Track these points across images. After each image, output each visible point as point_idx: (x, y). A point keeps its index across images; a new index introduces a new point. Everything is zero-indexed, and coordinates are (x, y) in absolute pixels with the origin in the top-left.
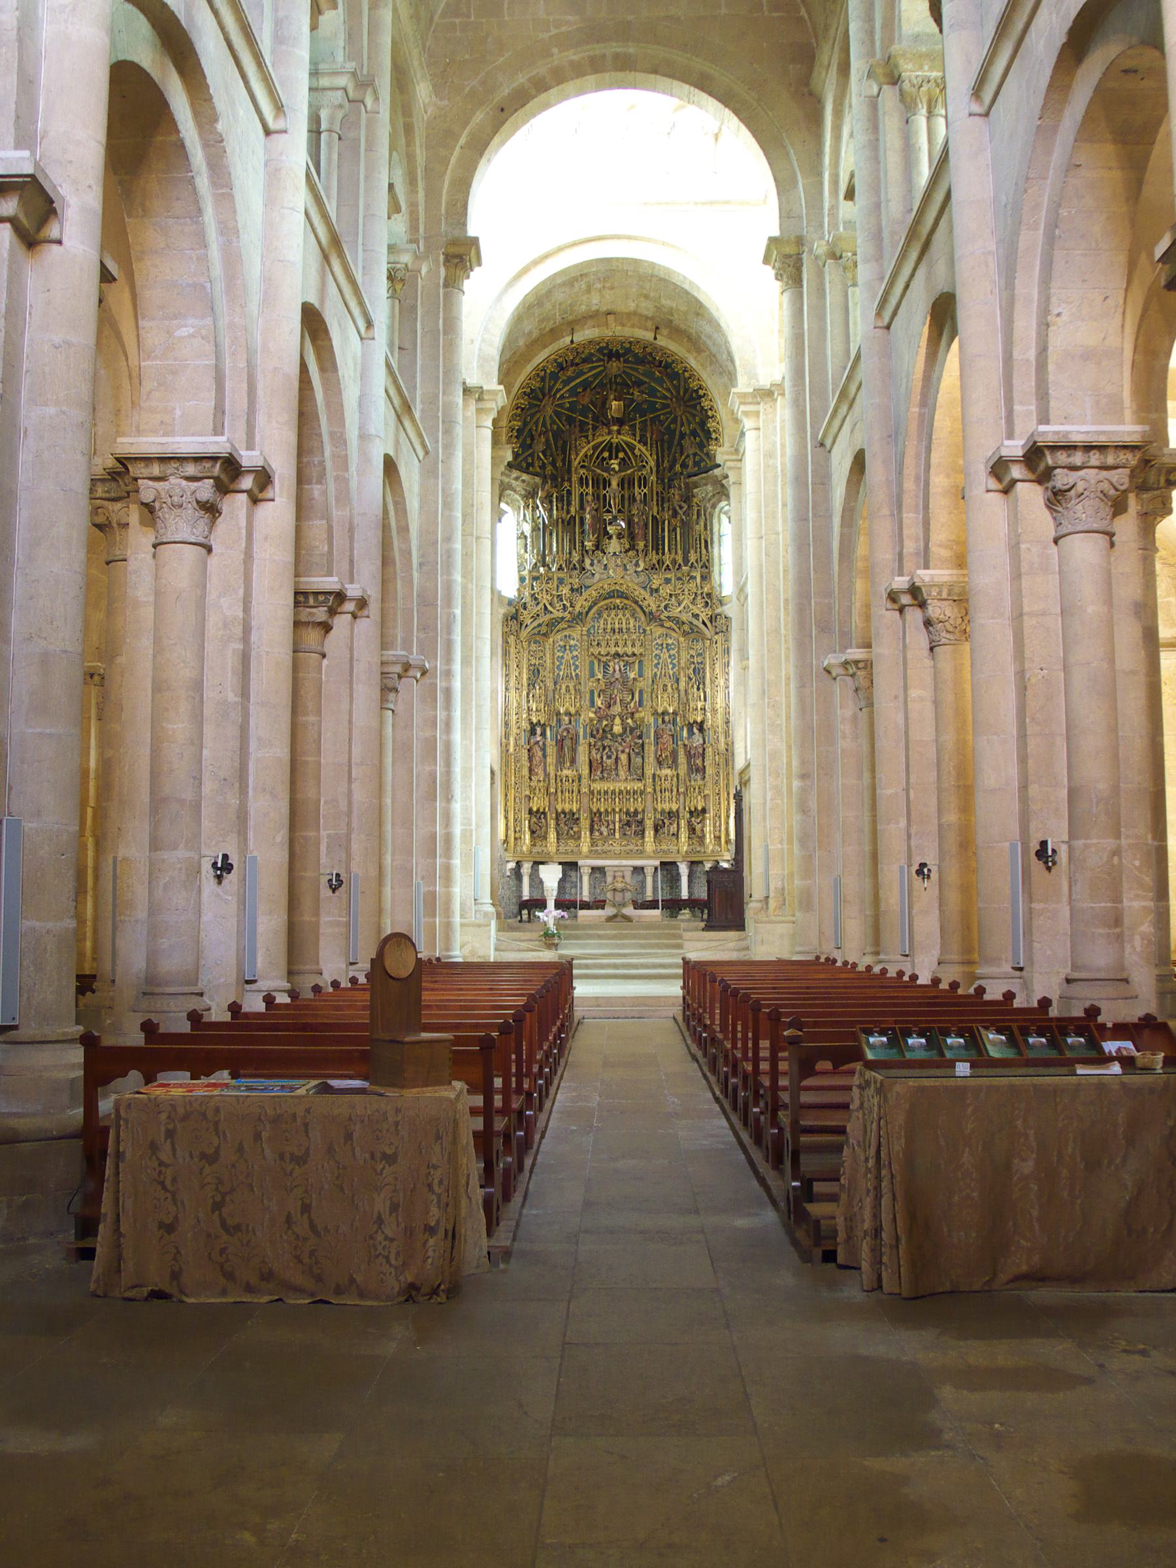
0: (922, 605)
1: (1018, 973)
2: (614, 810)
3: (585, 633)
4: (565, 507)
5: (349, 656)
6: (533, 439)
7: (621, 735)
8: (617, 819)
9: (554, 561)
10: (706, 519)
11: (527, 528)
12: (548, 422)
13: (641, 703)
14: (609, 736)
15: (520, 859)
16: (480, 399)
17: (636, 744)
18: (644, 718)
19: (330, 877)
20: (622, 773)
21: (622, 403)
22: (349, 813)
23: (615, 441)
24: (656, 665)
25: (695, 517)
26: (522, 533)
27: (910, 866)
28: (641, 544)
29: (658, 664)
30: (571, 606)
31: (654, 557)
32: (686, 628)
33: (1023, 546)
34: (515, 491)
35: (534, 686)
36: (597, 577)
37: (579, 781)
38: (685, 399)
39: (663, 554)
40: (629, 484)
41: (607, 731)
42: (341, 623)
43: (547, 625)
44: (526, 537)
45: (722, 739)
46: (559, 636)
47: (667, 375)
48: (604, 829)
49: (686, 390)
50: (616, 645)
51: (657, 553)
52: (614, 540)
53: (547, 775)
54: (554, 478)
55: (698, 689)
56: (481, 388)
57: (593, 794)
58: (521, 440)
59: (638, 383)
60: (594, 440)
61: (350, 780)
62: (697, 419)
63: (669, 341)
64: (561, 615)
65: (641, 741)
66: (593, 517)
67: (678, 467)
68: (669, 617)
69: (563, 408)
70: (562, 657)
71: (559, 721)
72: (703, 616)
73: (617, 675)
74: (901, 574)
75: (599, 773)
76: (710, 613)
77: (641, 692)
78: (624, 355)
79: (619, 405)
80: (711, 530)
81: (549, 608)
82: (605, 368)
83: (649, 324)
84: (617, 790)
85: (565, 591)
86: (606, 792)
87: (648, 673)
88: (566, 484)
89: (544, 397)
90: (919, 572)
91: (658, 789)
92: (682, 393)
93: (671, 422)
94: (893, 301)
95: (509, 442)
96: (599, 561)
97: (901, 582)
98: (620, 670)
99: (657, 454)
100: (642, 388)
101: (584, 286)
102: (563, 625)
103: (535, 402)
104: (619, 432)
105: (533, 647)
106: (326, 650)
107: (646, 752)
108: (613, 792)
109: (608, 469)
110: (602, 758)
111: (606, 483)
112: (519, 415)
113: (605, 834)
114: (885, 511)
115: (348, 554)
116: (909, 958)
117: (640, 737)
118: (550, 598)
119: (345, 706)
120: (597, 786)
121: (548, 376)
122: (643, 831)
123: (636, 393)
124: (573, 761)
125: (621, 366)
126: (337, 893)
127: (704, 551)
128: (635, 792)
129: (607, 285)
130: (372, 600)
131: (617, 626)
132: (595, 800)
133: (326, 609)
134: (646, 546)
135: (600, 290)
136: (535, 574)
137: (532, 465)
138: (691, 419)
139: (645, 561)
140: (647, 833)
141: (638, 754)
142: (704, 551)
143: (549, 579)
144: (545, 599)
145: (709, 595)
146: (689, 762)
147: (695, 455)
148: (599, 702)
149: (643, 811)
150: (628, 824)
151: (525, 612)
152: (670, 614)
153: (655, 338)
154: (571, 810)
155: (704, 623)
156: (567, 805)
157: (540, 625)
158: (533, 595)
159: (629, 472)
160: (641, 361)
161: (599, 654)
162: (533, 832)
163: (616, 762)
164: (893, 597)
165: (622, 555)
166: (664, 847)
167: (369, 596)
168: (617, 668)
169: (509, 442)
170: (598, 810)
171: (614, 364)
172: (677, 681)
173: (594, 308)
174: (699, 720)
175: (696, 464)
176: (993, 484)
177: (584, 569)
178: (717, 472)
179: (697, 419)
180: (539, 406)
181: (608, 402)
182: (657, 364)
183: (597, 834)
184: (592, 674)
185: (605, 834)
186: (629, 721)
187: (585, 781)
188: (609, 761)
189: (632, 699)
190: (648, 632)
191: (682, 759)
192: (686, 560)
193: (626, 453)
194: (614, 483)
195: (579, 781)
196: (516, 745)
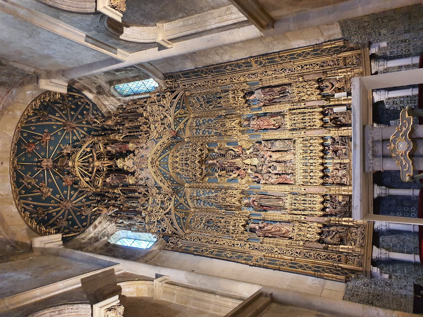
2: (322, 164)
8: (331, 161)
11: (126, 223)
14: (260, 168)
20: (288, 157)
29: (208, 131)
36: (148, 176)
38: (64, 121)
46: (190, 204)
47: (49, 132)
48: (340, 174)
50: (193, 162)
55: (220, 98)
64: (172, 203)
65: (263, 142)
73: (215, 161)
76: (168, 93)
77: (228, 144)
81: (167, 211)
85: (159, 198)
87: (214, 139)
92: (61, 123)
96: (140, 175)
98: (213, 159)
100: (63, 148)
102: (182, 200)
105: (193, 224)
110: (276, 174)
113: (344, 172)
117: (260, 143)
118: (161, 211)
124: (279, 198)
132: (311, 181)
147: (93, 114)
149: (322, 138)
150: (335, 152)
155: (175, 98)
156: (316, 206)
161: (201, 174)
162: (342, 241)
163: (279, 162)
186: (248, 152)
187: (295, 189)
188: (279, 168)
189: (232, 150)
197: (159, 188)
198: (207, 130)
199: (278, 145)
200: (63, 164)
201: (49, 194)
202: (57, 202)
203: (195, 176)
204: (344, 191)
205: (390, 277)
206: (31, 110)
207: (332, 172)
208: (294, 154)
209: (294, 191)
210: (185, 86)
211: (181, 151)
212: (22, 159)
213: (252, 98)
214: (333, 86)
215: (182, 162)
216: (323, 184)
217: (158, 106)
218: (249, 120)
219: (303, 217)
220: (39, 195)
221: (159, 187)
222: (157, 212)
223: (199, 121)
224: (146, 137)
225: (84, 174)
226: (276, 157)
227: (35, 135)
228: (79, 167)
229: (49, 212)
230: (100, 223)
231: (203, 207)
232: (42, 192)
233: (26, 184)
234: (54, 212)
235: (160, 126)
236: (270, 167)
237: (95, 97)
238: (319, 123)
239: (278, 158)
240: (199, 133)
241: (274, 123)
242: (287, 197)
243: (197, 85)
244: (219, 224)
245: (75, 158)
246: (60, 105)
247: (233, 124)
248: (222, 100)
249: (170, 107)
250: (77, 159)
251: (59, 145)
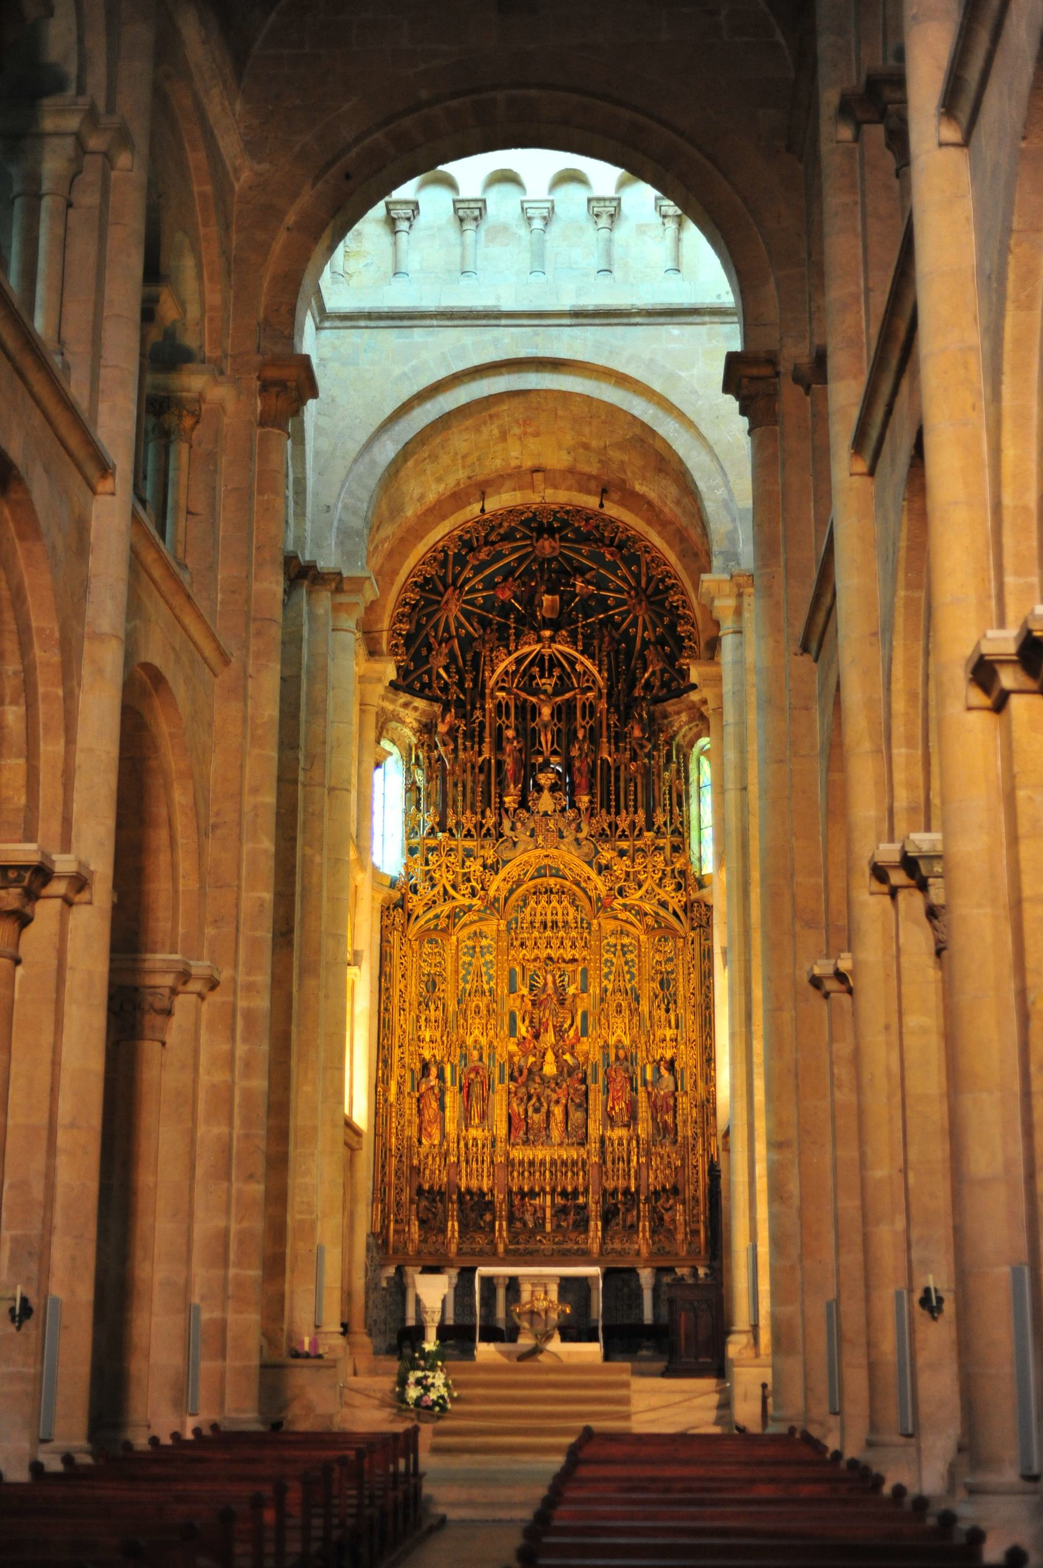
0: (923, 886)
1: (1030, 1486)
2: (543, 1189)
3: (502, 927)
4: (476, 747)
5: (55, 962)
6: (430, 649)
7: (555, 1078)
9: (458, 824)
10: (679, 763)
13: (585, 1032)
15: (402, 1263)
16: (338, 590)
17: (576, 1090)
18: (588, 1053)
19: (11, 1303)
20: (556, 1134)
21: (557, 597)
22: (49, 1203)
23: (546, 651)
24: (606, 976)
25: (662, 761)
26: (414, 783)
27: (911, 1291)
28: (586, 799)
29: (610, 972)
30: (483, 889)
31: (603, 820)
32: (650, 920)
33: (1021, 794)
34: (403, 722)
35: (427, 1005)
36: (521, 847)
37: (493, 1146)
38: (649, 592)
39: (618, 813)
40: (568, 714)
41: (533, 1073)
42: (46, 911)
43: (448, 917)
44: (419, 789)
45: (701, 1084)
46: (466, 932)
47: (623, 558)
49: (650, 579)
50: (549, 945)
51: (609, 813)
52: (546, 795)
53: (444, 1135)
54: (460, 704)
55: (667, 1011)
56: (340, 574)
57: (513, 1166)
58: (412, 650)
59: (582, 571)
60: (517, 649)
61: (51, 1150)
62: (666, 620)
63: (622, 509)
64: (467, 902)
65: (583, 1087)
66: (516, 761)
67: (638, 692)
68: (624, 906)
69: (473, 605)
70: (470, 964)
71: (464, 1057)
72: (674, 904)
73: (550, 990)
74: (891, 840)
75: (521, 1133)
76: (685, 899)
77: (585, 1015)
78: (560, 530)
79: (553, 601)
80: (687, 778)
81: (451, 892)
82: (534, 548)
83: (593, 484)
84: (548, 1159)
85: (474, 866)
86: (532, 1163)
87: (594, 989)
88: (478, 713)
89: (446, 588)
90: (914, 836)
91: (609, 1158)
93: (630, 626)
94: (874, 434)
95: (393, 651)
96: (523, 824)
97: (889, 853)
99: (609, 670)
100: (588, 576)
101: (496, 432)
103: (434, 597)
104: (552, 639)
105: (427, 948)
106: (22, 953)
107: (590, 1102)
108: (542, 1163)
109: (536, 692)
110: (526, 1111)
111: (535, 711)
112: (409, 616)
113: (531, 1225)
114: (867, 745)
115: (60, 809)
116: (913, 1440)
117: (583, 1081)
118: (451, 877)
119: (47, 1038)
120: (517, 1154)
121: (451, 559)
122: (587, 1221)
124: (483, 1116)
125: (556, 545)
126: (23, 1329)
127: (676, 810)
128: (574, 1163)
129: (530, 430)
130: (97, 878)
131: (549, 918)
132: (515, 1174)
133: (19, 890)
134: (591, 802)
135: (520, 439)
136: (432, 843)
137: (429, 686)
139: (590, 824)
140: (592, 1223)
141: (579, 1106)
142: (676, 810)
143: (451, 850)
144: (444, 879)
145: (683, 873)
146: (654, 1119)
148: (523, 1029)
151: (415, 898)
152: (628, 901)
153: (601, 506)
154: (480, 1189)
155: (675, 913)
157: (437, 917)
158: (429, 871)
159: (567, 696)
160: (583, 538)
162: (422, 1222)
164: (879, 873)
165: (557, 815)
166: (617, 1245)
167: (92, 873)
168: (549, 978)
169: (393, 651)
170: (521, 1189)
171: (547, 544)
172: (637, 999)
173: (514, 463)
174: (668, 1055)
175: (664, 684)
176: (978, 697)
177: (501, 835)
178: (694, 696)
179: (666, 620)
180: (439, 602)
181: (537, 596)
182: (607, 542)
183: (518, 1224)
184: (512, 990)
185: (531, 1225)
186: (567, 1057)
189: (571, 1025)
190: (595, 927)
191: (644, 1111)
192: (650, 824)
194: (546, 711)
195: (493, 1146)
196: (400, 1092)
197: (495, 868)
198: (613, 969)
199: (577, 1116)
203: (522, 944)
204: (501, 1225)
205: (384, 1289)
207: (531, 1205)
208: (561, 1144)
209: (499, 1145)
210: (692, 943)
211: (571, 910)
213: (663, 1071)
214: (667, 1210)
215: (549, 914)
216: (510, 1192)
217: (664, 871)
218: (626, 1058)
219: (456, 1159)
221: (498, 869)
222: (447, 867)
223: (631, 952)
224: (603, 829)
226: (556, 1112)
230: (416, 709)
231: (461, 962)
235: (624, 868)
236: (539, 1099)
237: (693, 702)
238: (610, 1185)
239: (554, 1115)
240: (607, 951)
241: (617, 1108)
242: (486, 1131)
243: (692, 969)
244: (432, 1007)
245: (560, 643)
247: (619, 1031)
248: (663, 1012)
249: (659, 900)
251: (592, 569)
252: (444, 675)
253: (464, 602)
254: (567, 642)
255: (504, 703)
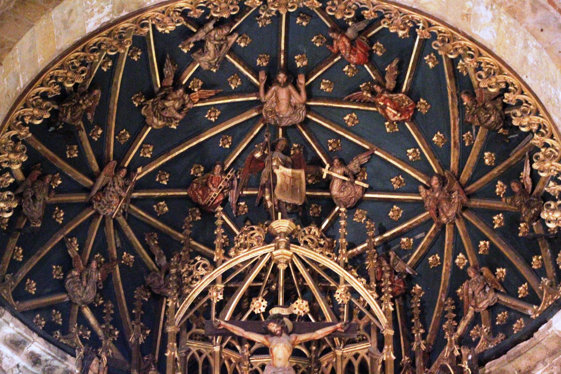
12: (113, 243)
38: (464, 177)
62: (498, 220)
78: (308, 72)
79: (294, 178)
89: (102, 165)
100: (354, 166)
104: (293, 239)
123: (337, 174)
137: (65, 330)
138: (480, 226)
147: (493, 309)
171: (283, 94)
179: (498, 220)
193: (312, 301)
200: (282, 191)
201: (155, 120)
202: (120, 155)
206: (498, 84)
212: (302, 18)
220: (152, 84)
225: (242, 278)
227: (402, 68)
228: (266, 258)
229: (83, 134)
232: (165, 98)
233: (201, 35)
234: (81, 150)
245: (306, 243)
246: (528, 181)
250: (302, 251)
252: (92, 320)
253: (134, 201)
254: (321, 246)
255: (200, 361)
